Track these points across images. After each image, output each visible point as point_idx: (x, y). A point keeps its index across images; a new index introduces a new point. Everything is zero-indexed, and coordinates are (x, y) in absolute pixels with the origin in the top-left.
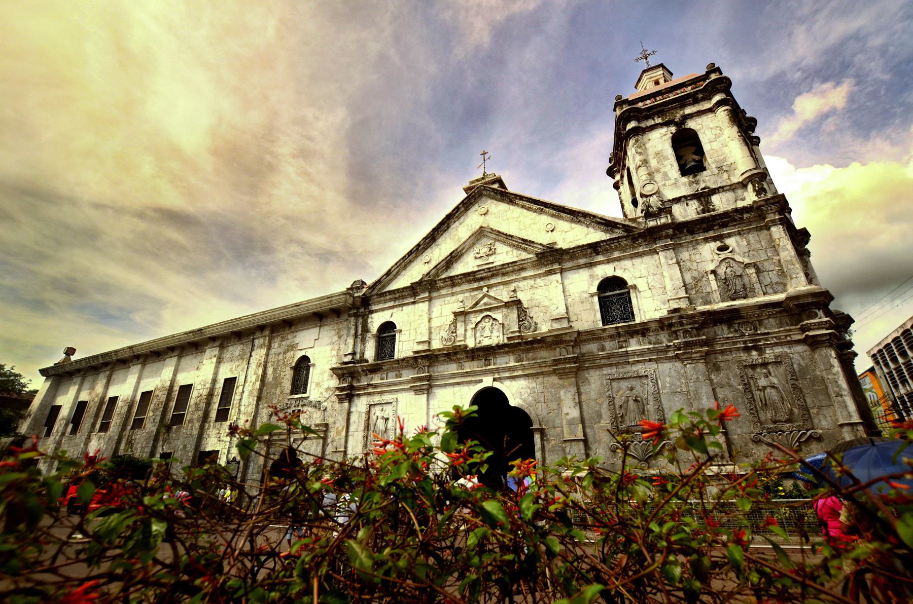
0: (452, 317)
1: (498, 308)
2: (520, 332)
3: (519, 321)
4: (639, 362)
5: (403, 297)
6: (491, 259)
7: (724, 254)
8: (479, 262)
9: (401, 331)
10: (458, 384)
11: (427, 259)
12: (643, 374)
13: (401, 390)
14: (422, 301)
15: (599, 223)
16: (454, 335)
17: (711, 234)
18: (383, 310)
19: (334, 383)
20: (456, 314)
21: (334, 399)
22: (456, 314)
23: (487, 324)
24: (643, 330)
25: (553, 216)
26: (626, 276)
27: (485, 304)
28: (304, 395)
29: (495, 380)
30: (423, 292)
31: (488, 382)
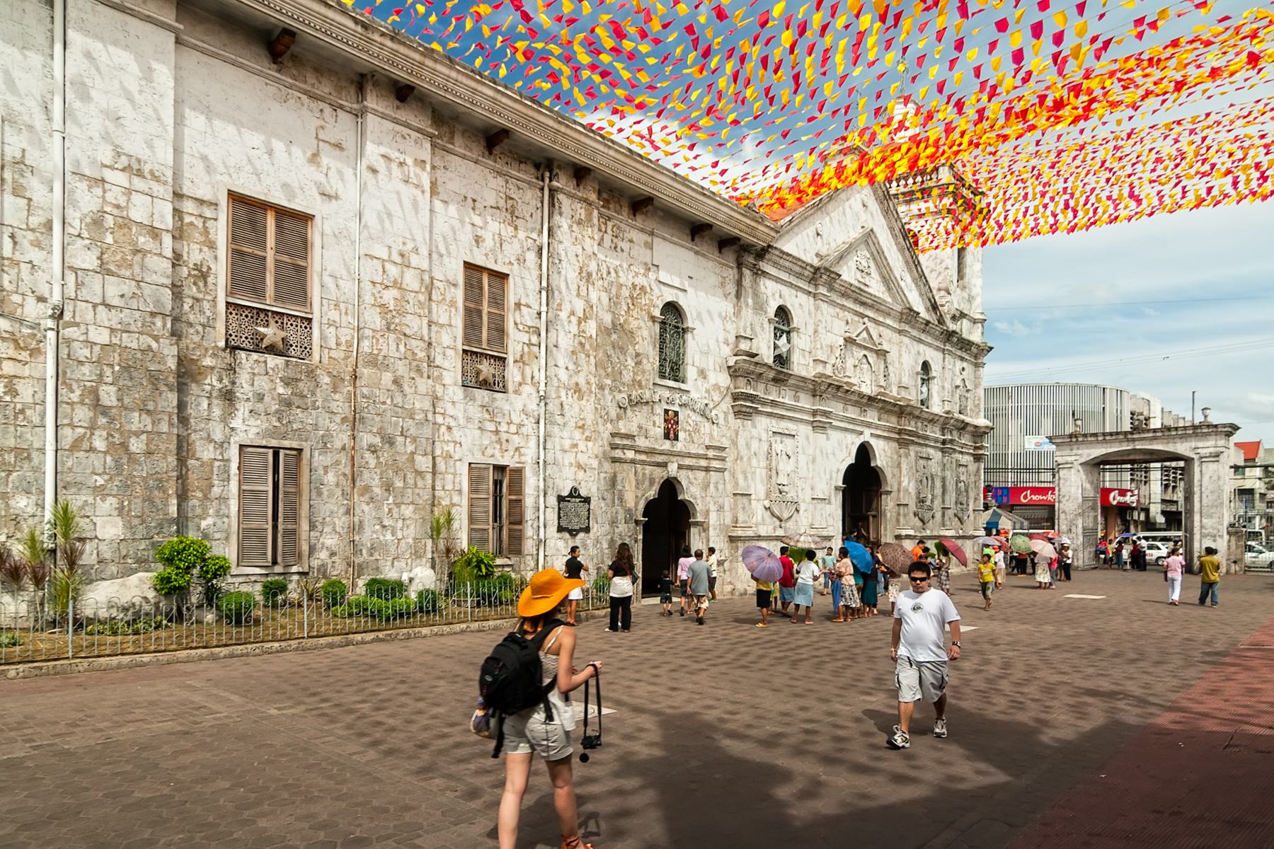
0: (842, 342)
5: (799, 276)
10: (846, 430)
13: (802, 421)
15: (930, 300)
17: (959, 353)
18: (778, 280)
19: (724, 380)
20: (849, 341)
21: (727, 404)
23: (866, 366)
24: (932, 420)
25: (907, 262)
27: (864, 339)
28: (683, 386)
31: (867, 436)
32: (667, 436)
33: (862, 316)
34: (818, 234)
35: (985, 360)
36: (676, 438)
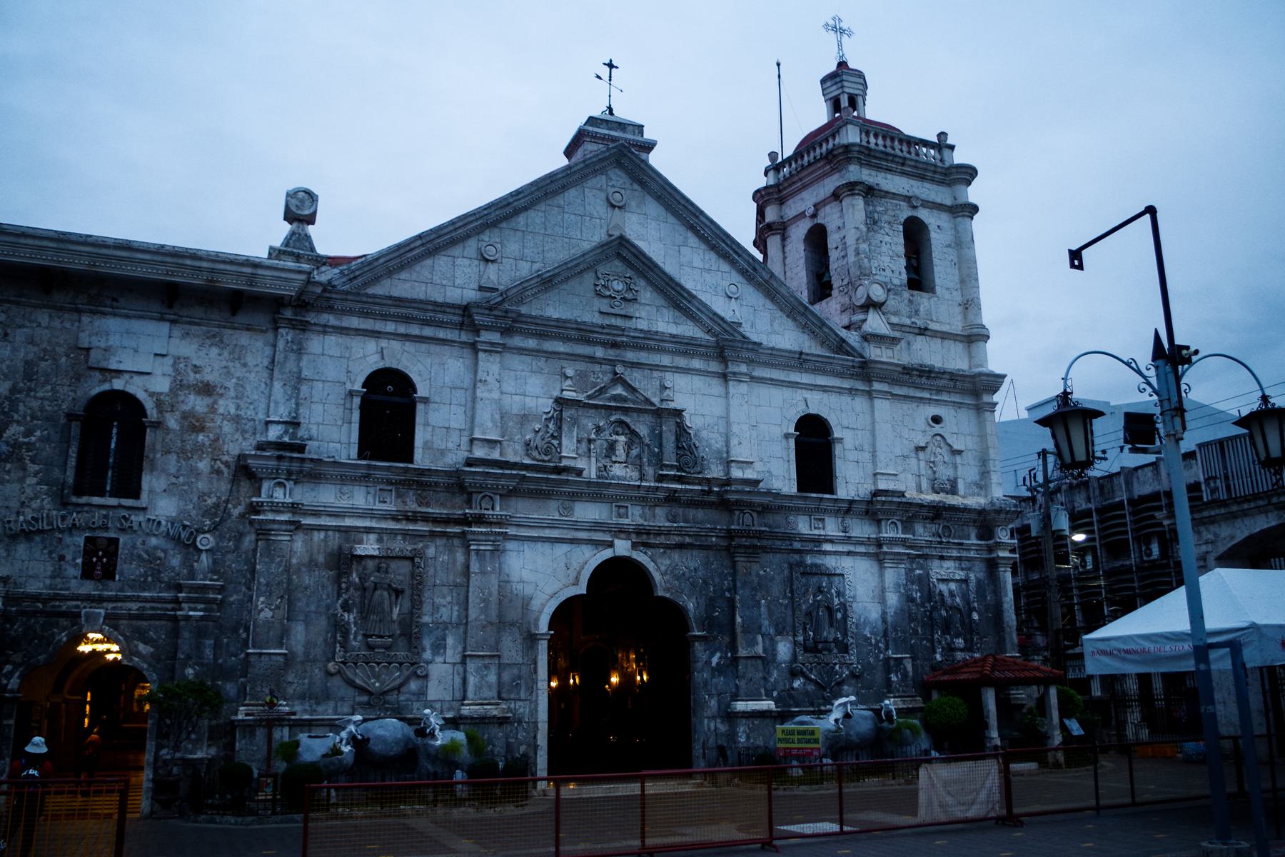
1: (640, 411)
2: (679, 469)
3: (678, 448)
4: (836, 553)
6: (631, 309)
7: (938, 429)
8: (604, 305)
9: (426, 400)
11: (491, 252)
12: (838, 572)
14: (493, 349)
16: (555, 442)
20: (560, 402)
22: (560, 402)
26: (833, 421)
29: (635, 546)
30: (489, 328)
31: (622, 547)
32: (87, 573)
33: (612, 363)
34: (487, 261)
35: (996, 397)
36: (109, 574)
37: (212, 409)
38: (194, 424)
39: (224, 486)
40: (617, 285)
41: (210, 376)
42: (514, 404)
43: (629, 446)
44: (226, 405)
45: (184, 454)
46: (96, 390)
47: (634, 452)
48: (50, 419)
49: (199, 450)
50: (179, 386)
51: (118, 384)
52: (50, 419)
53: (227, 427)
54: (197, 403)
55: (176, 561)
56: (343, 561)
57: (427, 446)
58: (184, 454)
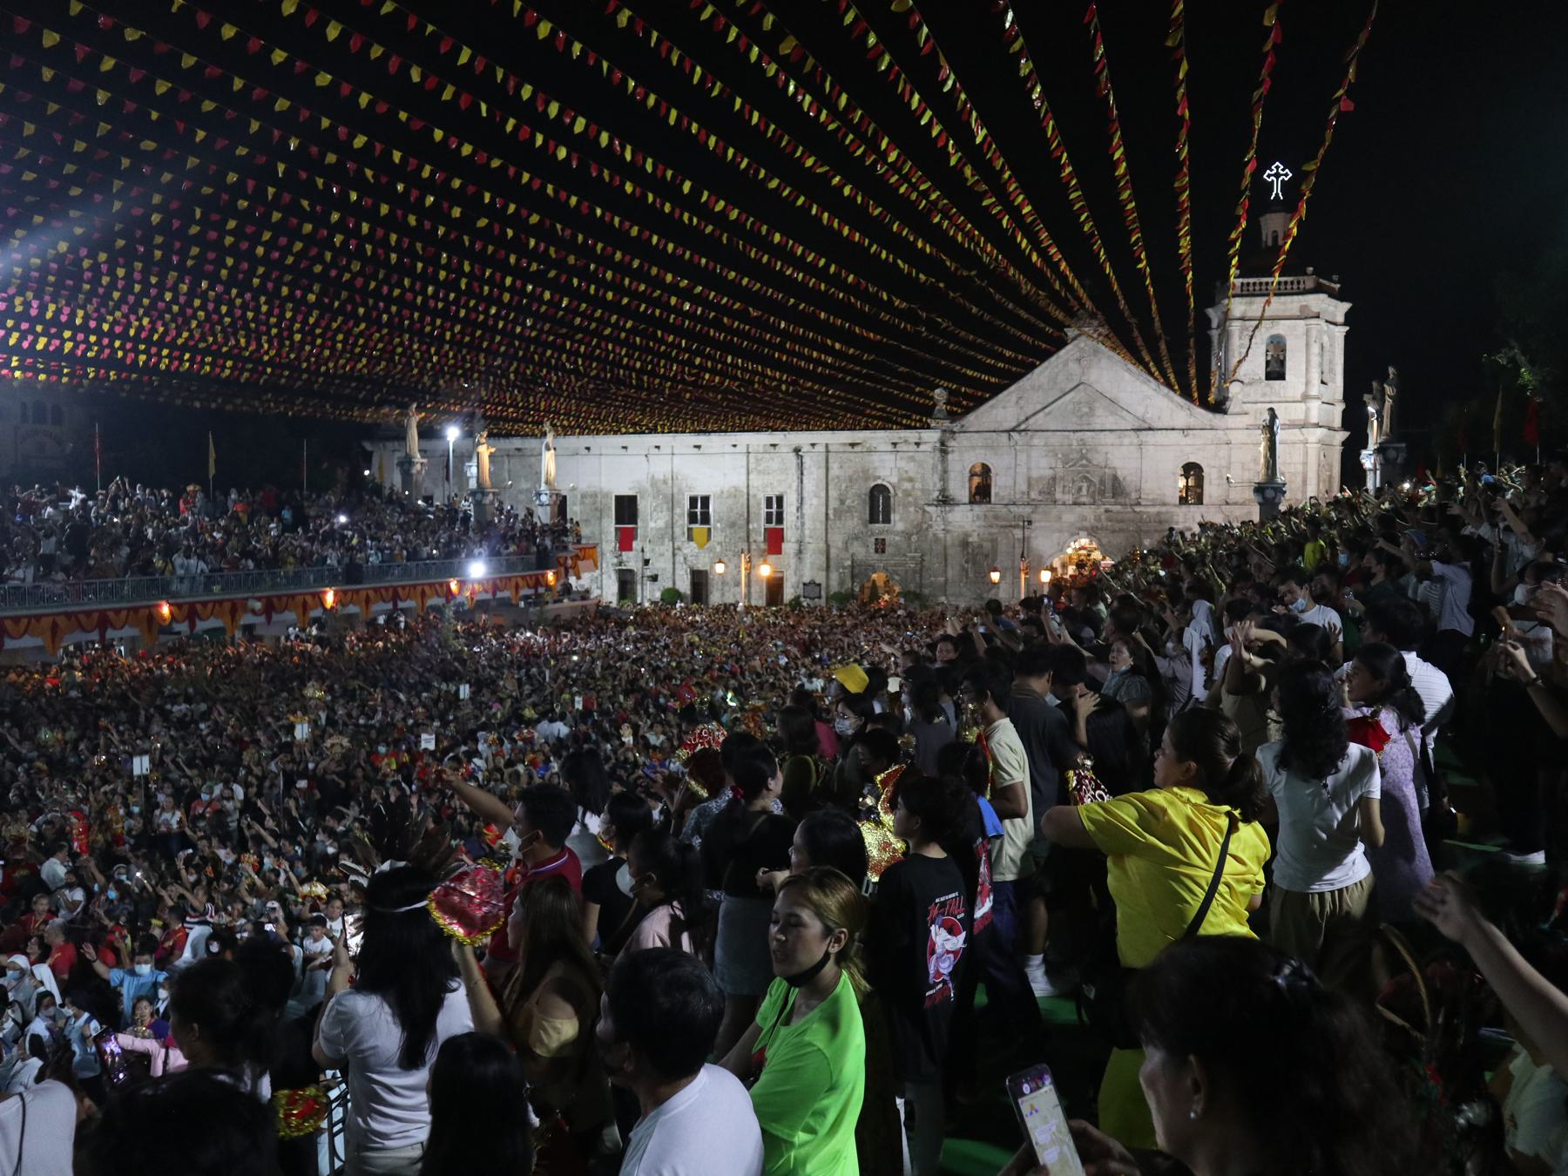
32: (876, 551)
36: (883, 551)
37: (913, 488)
38: (907, 494)
39: (920, 516)
40: (1086, 410)
41: (911, 474)
42: (1035, 474)
43: (1089, 487)
44: (918, 485)
45: (906, 506)
46: (873, 484)
47: (1092, 489)
48: (859, 496)
49: (910, 503)
50: (901, 480)
51: (879, 482)
52: (859, 496)
53: (919, 493)
54: (907, 485)
55: (904, 546)
56: (965, 544)
57: (997, 494)
58: (906, 506)
